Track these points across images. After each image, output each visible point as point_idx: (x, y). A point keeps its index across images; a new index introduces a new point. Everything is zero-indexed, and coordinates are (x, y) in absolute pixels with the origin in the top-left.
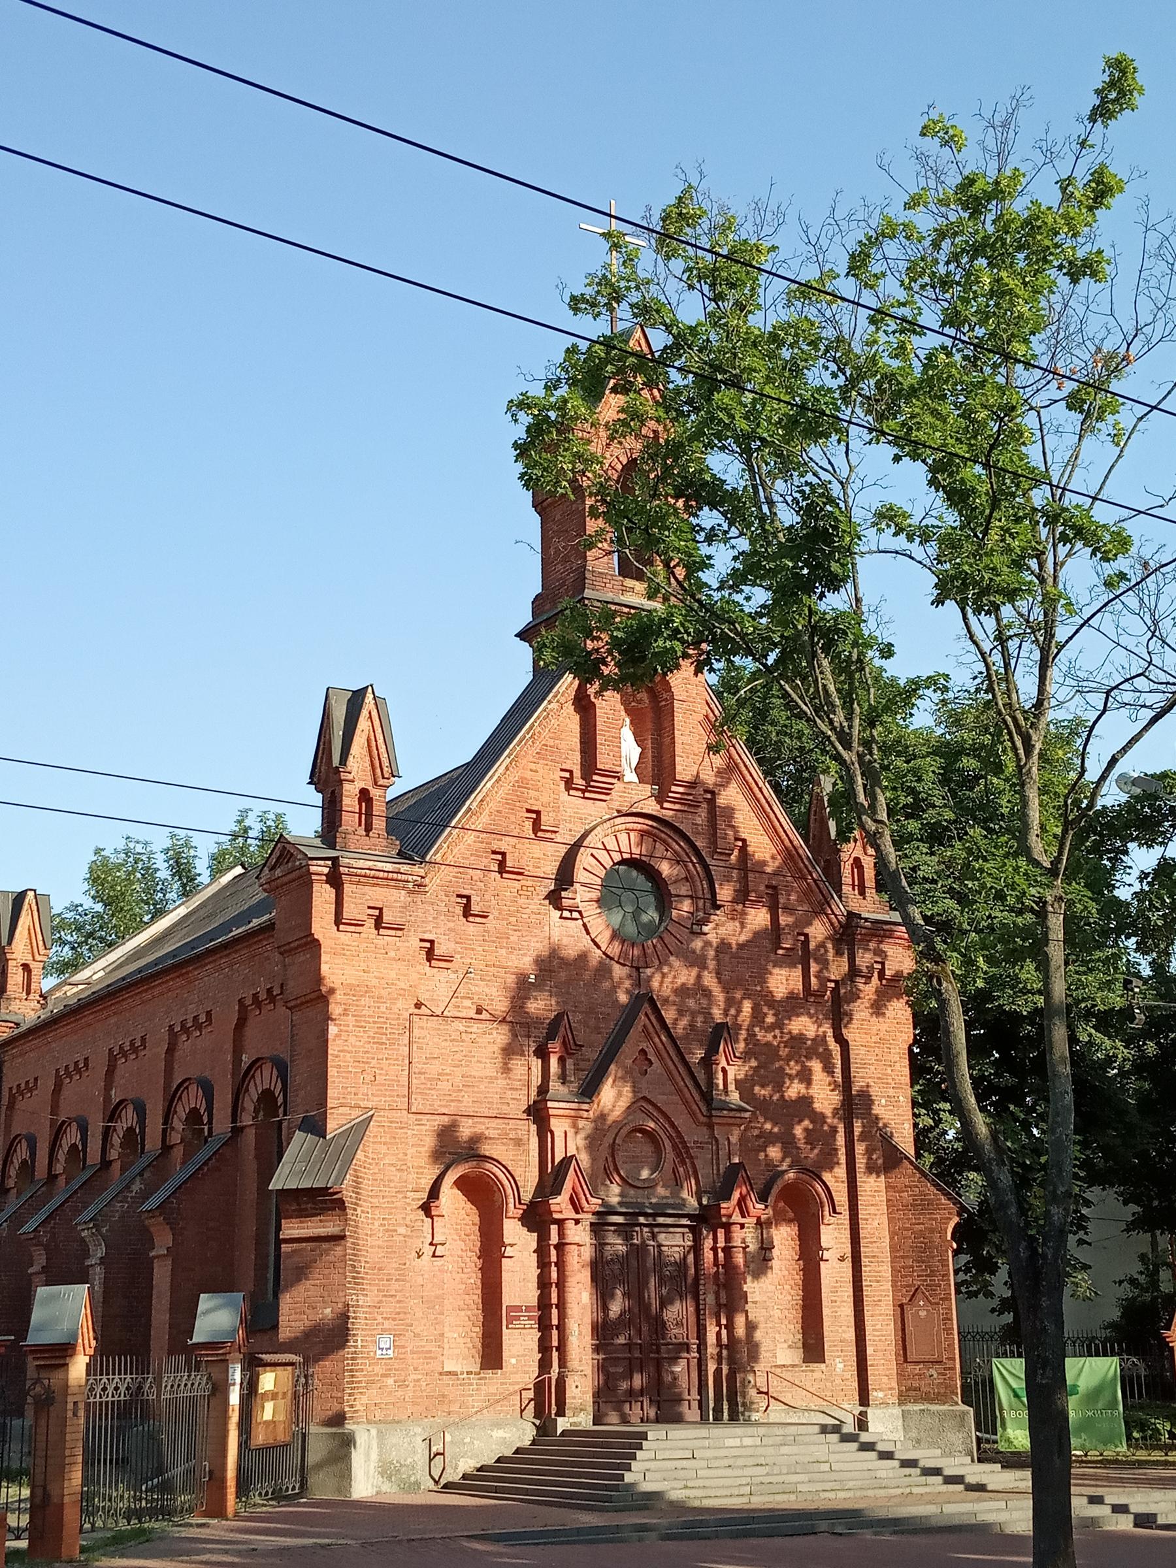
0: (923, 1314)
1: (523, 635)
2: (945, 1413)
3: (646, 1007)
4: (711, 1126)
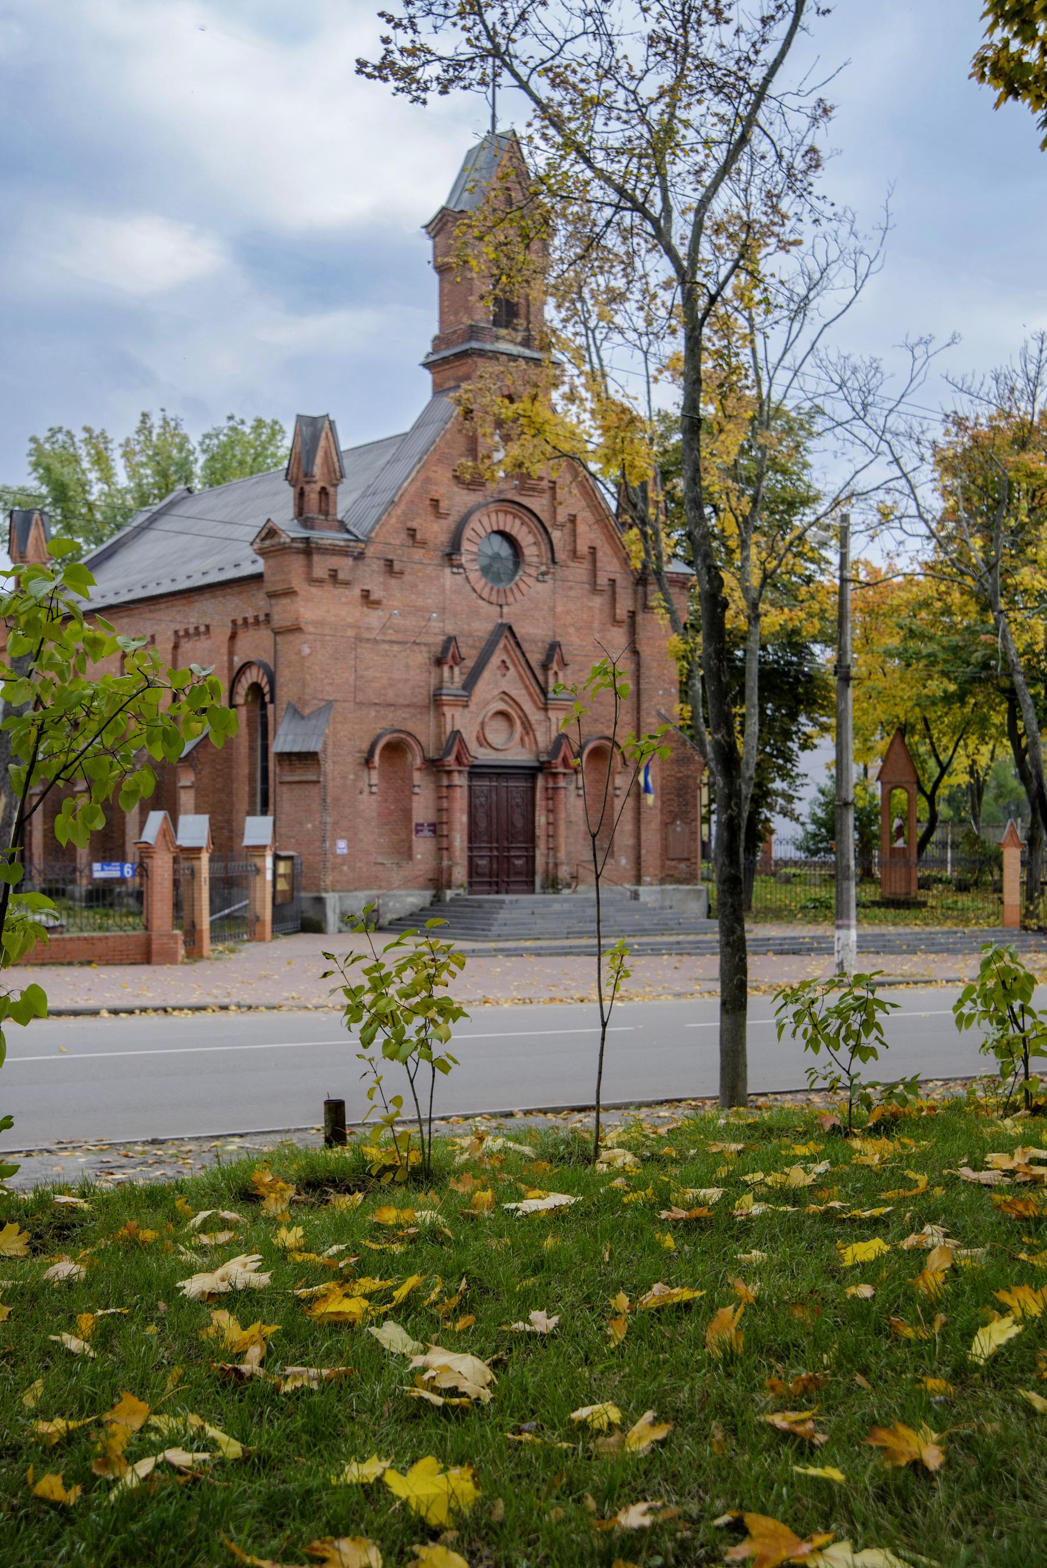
0: (679, 829)
1: (426, 365)
2: (689, 891)
3: (507, 633)
4: (546, 710)
